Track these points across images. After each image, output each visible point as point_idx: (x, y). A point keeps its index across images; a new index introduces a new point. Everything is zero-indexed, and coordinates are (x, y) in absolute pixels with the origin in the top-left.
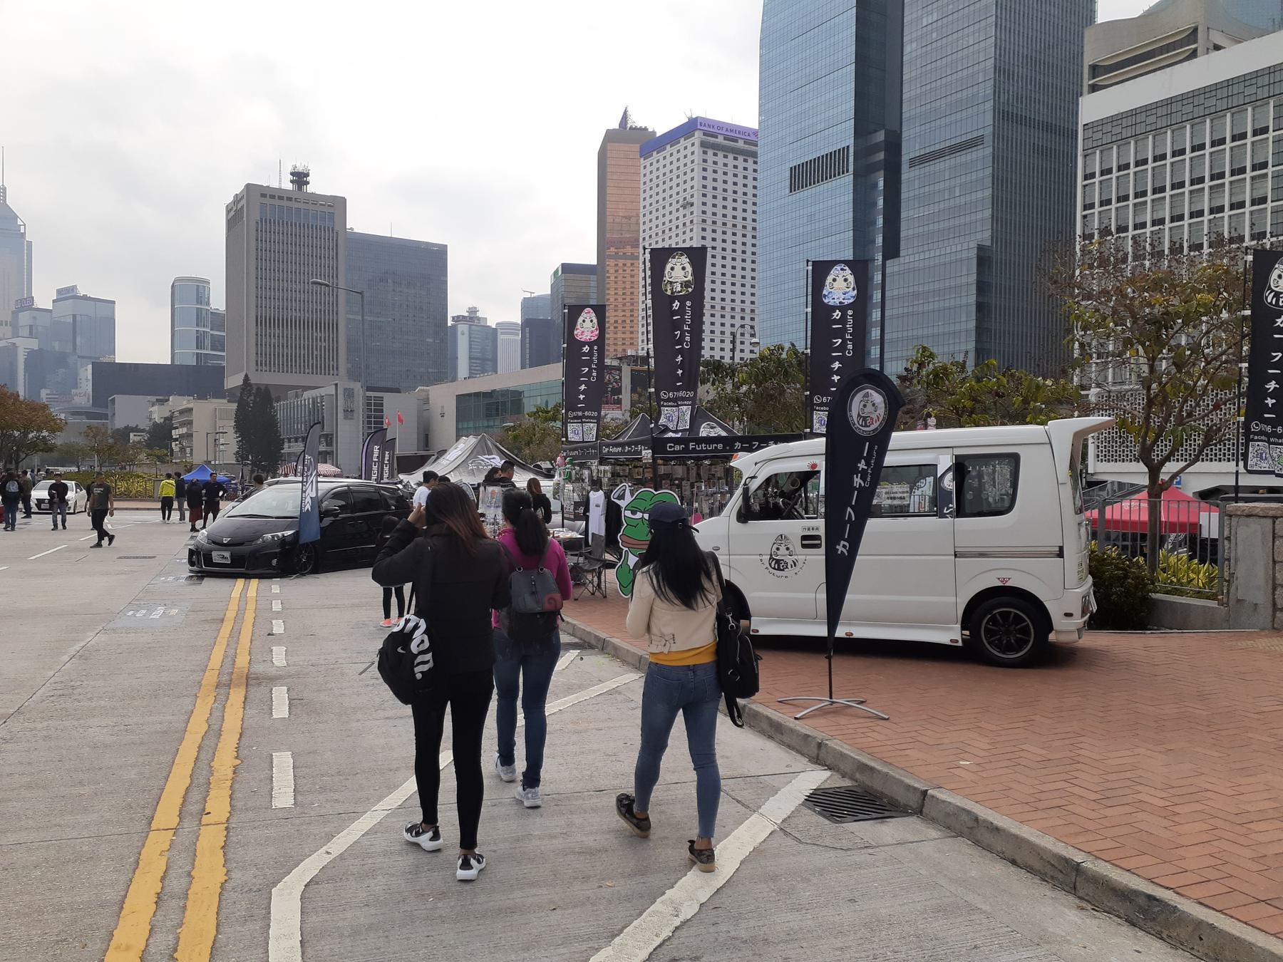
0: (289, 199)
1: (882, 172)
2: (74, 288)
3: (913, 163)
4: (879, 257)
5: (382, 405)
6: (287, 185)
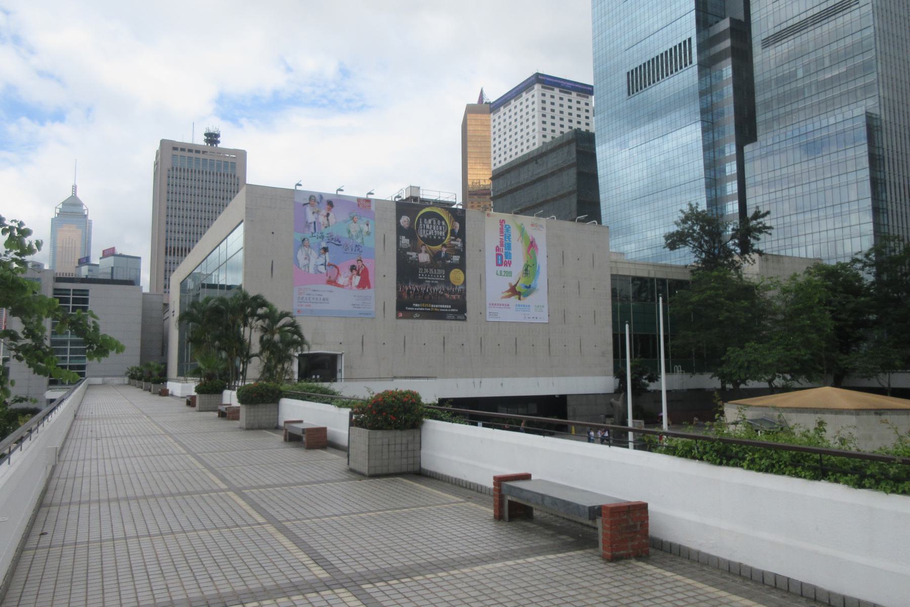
0: (198, 152)
1: (729, 60)
2: (113, 249)
3: (767, 43)
4: (731, 149)
5: (86, 301)
6: (200, 140)
